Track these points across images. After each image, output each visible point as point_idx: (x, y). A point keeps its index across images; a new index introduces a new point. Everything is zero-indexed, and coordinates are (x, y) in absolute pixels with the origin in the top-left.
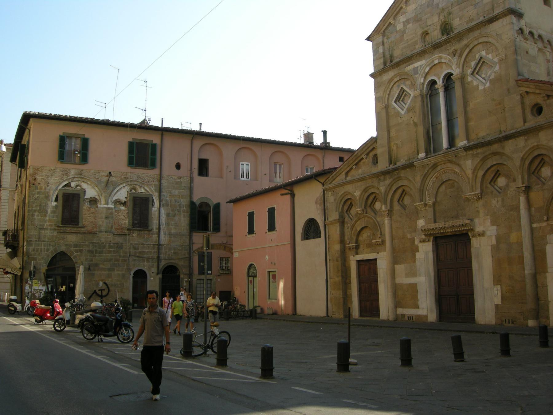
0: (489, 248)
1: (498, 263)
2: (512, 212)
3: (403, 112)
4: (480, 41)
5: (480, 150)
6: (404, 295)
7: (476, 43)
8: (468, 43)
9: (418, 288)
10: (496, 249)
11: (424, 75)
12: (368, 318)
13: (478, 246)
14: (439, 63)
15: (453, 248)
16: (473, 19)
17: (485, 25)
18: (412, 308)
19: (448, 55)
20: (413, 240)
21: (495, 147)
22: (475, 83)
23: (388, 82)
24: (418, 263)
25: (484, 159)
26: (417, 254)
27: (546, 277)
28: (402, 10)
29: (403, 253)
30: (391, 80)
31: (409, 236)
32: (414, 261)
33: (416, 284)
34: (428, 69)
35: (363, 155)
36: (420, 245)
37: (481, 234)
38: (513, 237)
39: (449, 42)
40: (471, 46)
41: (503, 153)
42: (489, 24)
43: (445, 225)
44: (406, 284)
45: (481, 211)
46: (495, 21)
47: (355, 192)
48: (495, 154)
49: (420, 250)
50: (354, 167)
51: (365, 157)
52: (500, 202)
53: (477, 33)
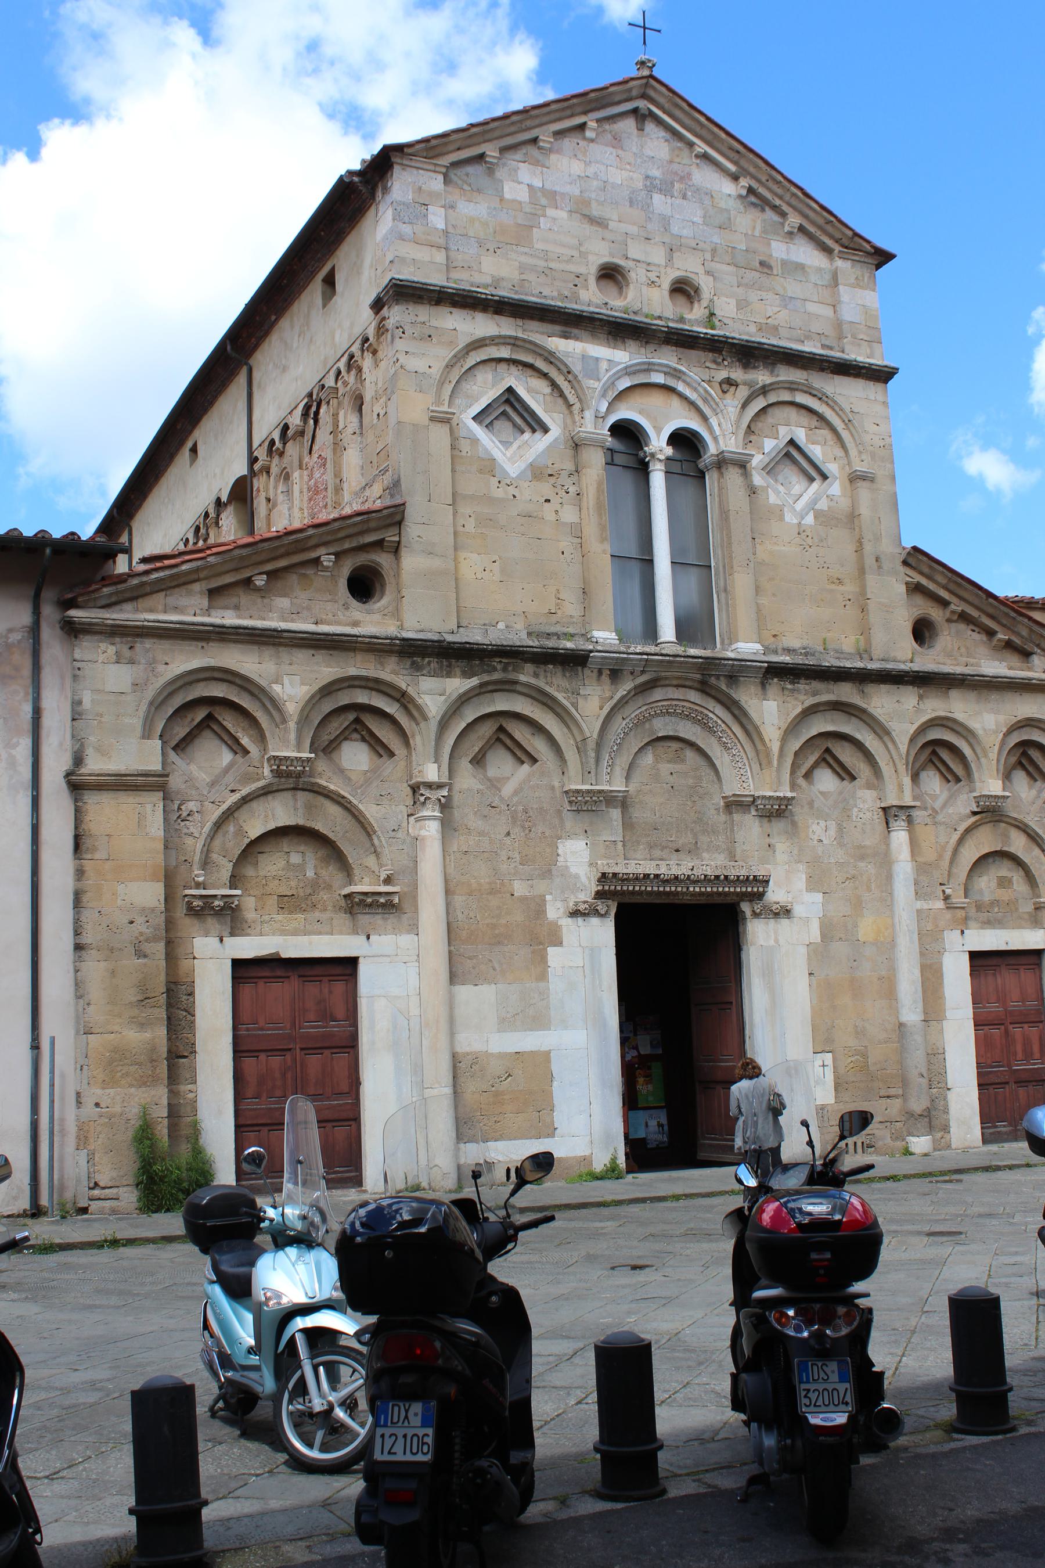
0: (803, 950)
1: (827, 994)
2: (862, 864)
4: (801, 398)
7: (786, 396)
8: (771, 384)
9: (555, 1067)
10: (819, 953)
11: (611, 395)
13: (772, 942)
16: (776, 328)
20: (538, 908)
21: (846, 692)
22: (773, 499)
23: (468, 345)
24: (555, 984)
25: (808, 713)
28: (532, 150)
31: (520, 888)
32: (543, 976)
33: (547, 1055)
34: (625, 383)
35: (321, 551)
38: (867, 928)
40: (772, 398)
41: (864, 711)
42: (833, 372)
44: (502, 1056)
48: (839, 707)
50: (260, 581)
51: (327, 560)
52: (832, 832)
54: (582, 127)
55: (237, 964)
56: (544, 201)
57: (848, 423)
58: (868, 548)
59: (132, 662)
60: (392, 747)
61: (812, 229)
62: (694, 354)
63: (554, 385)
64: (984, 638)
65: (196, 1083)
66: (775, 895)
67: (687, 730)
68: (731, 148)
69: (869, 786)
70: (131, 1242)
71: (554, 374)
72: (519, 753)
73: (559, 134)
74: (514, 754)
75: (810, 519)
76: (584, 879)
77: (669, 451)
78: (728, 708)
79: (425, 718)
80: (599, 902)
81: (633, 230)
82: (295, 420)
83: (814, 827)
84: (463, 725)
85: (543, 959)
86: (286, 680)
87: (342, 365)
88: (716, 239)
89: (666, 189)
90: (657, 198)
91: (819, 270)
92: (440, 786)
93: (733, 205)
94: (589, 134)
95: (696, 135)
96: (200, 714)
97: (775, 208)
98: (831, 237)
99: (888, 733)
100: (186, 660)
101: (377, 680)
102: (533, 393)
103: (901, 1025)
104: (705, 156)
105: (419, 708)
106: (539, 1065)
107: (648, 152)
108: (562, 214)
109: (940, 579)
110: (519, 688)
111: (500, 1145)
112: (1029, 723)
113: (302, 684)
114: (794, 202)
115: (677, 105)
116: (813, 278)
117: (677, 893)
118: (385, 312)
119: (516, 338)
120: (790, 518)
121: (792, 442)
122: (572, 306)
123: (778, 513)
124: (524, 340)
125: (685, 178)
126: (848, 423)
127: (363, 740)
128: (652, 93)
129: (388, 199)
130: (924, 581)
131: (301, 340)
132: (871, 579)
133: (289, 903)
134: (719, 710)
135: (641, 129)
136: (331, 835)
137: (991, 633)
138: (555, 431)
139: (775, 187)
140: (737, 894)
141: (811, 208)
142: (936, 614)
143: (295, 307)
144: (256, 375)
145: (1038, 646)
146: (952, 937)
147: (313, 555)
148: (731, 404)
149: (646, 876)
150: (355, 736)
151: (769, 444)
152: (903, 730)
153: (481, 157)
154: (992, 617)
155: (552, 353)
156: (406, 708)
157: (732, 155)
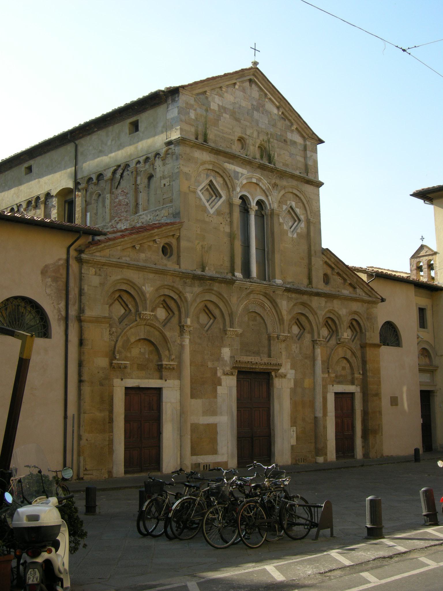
0: (289, 390)
2: (306, 360)
3: (212, 211)
4: (295, 191)
5: (294, 295)
6: (203, 438)
10: (293, 391)
12: (136, 475)
13: (280, 387)
14: (256, 183)
15: (256, 384)
17: (302, 182)
18: (209, 454)
19: (269, 184)
21: (305, 298)
24: (219, 400)
26: (219, 387)
27: (326, 420)
29: (203, 385)
30: (204, 163)
32: (216, 397)
36: (223, 378)
37: (284, 376)
38: (307, 383)
39: (272, 172)
41: (310, 306)
43: (257, 361)
44: (203, 425)
45: (284, 353)
46: (309, 184)
47: (144, 285)
49: (223, 383)
52: (298, 349)
53: (295, 183)
54: (235, 84)
55: (127, 389)
56: (222, 111)
57: (308, 202)
58: (312, 248)
59: (100, 275)
60: (174, 311)
61: (300, 129)
62: (265, 172)
63: (224, 180)
64: (342, 281)
65: (113, 432)
66: (282, 370)
67: (259, 310)
68: (279, 97)
69: (309, 333)
70: (125, 488)
71: (225, 177)
72: (210, 315)
73: (228, 86)
74: (208, 315)
75: (295, 236)
76: (228, 362)
77: (256, 208)
78: (271, 302)
79: (186, 301)
80: (233, 370)
81: (248, 124)
82: (108, 174)
83: (293, 347)
84: (196, 305)
85: (216, 391)
86: (146, 286)
87: (142, 160)
88: (272, 130)
89: (257, 110)
90: (255, 112)
91: (301, 144)
92: (190, 326)
93: (276, 117)
94: (237, 87)
95: (267, 90)
96: (117, 295)
97: (289, 120)
98: (305, 133)
99: (316, 314)
100: (116, 275)
101: (173, 287)
102: (218, 183)
103: (316, 418)
104: (270, 99)
105: (185, 298)
106: (212, 429)
107: (253, 96)
108: (228, 116)
109: (332, 260)
110: (213, 292)
111: (202, 457)
112: (356, 313)
113: (151, 287)
114: (296, 119)
115: (263, 80)
116: (299, 147)
117: (256, 368)
118: (172, 146)
119: (215, 162)
120: (290, 235)
121: (291, 207)
122: (228, 150)
123: (286, 232)
124: (217, 163)
125: (263, 106)
126: (308, 202)
127: (164, 307)
128: (256, 74)
129: (176, 105)
130: (328, 261)
131: (113, 142)
132: (313, 259)
133: (142, 367)
134: (269, 303)
135: (251, 86)
136: (155, 343)
137: (345, 280)
138: (224, 198)
139: (290, 113)
140: (272, 369)
141: (301, 122)
142: (329, 271)
143: (110, 128)
144: (80, 149)
145: (358, 286)
146: (330, 387)
147: (154, 239)
148: (275, 193)
149: (248, 362)
150: (161, 306)
151: (285, 207)
152: (322, 314)
153: (205, 92)
154: (347, 275)
155: (225, 169)
156: (180, 297)
157: (279, 100)
